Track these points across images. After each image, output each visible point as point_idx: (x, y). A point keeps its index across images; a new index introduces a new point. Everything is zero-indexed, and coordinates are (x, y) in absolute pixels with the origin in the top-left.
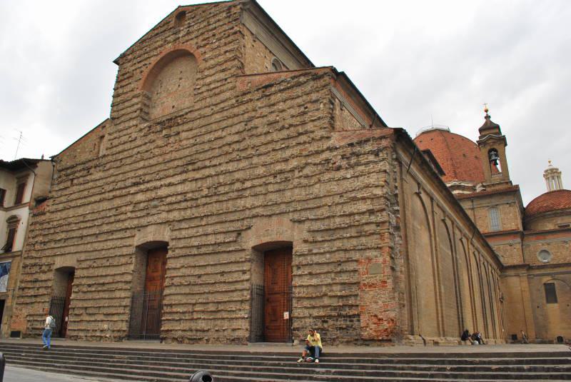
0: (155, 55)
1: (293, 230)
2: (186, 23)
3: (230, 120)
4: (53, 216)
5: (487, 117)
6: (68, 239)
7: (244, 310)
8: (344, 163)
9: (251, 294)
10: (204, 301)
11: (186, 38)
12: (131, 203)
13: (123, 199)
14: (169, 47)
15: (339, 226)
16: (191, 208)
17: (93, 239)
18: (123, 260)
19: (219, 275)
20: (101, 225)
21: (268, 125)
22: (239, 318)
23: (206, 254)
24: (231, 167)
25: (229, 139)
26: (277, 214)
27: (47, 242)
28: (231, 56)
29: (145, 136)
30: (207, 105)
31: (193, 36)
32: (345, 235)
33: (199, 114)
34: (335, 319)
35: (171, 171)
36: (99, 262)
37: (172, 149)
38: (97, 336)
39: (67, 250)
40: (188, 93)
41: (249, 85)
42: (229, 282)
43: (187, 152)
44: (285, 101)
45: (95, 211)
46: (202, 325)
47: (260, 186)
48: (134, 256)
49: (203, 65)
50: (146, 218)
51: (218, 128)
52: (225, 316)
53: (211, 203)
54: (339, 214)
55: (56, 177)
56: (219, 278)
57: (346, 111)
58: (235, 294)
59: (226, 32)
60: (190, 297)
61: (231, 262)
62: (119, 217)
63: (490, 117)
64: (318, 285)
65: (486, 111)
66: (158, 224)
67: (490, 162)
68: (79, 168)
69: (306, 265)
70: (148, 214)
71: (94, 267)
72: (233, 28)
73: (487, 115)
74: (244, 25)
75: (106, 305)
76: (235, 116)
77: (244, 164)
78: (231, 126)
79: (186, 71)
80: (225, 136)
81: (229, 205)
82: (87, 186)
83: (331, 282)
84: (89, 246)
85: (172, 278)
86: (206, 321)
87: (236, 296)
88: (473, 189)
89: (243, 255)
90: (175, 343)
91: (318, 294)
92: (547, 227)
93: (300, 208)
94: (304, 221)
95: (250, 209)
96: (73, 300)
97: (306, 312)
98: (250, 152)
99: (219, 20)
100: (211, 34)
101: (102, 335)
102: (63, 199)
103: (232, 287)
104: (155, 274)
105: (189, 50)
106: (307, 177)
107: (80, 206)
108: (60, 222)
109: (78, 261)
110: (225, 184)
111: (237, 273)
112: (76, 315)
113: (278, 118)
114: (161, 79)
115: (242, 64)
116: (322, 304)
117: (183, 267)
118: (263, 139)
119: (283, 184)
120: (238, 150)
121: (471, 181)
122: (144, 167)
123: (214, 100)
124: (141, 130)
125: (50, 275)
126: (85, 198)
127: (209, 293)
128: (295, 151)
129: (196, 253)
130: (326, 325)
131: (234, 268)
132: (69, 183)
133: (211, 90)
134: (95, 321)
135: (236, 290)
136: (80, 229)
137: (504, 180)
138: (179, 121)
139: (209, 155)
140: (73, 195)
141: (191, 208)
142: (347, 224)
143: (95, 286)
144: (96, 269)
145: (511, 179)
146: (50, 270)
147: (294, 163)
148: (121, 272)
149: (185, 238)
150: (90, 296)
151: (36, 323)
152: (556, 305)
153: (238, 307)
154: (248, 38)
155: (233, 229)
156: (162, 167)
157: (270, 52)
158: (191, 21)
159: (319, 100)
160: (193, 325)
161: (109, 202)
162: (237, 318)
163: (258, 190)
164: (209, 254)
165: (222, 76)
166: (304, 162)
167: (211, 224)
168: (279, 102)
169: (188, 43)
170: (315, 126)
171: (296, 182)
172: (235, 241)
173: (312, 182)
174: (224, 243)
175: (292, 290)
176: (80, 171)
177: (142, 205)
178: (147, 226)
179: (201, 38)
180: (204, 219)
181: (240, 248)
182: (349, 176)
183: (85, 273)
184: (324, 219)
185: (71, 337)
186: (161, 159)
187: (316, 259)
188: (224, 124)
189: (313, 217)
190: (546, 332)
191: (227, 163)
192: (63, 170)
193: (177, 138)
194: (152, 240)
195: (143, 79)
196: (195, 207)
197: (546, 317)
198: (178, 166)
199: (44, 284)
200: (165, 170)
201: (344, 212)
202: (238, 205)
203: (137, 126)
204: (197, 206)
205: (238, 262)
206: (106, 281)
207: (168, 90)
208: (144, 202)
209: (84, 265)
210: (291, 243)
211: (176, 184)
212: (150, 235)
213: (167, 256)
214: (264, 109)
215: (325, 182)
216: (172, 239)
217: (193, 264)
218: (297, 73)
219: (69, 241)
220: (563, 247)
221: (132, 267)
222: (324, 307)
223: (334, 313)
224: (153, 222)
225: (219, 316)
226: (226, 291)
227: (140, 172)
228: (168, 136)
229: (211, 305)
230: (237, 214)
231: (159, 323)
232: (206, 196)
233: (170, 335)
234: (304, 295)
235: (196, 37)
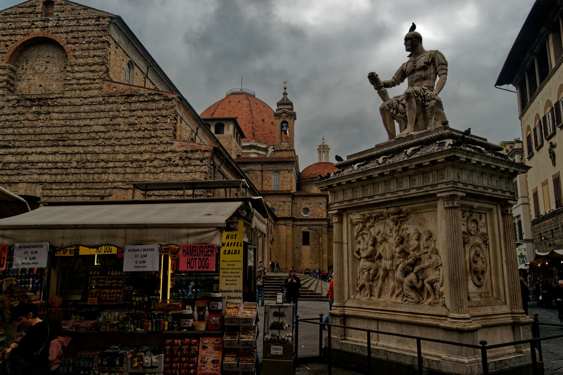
0: (21, 35)
2: (55, 14)
3: (98, 113)
5: (285, 94)
8: (181, 163)
11: (55, 30)
14: (37, 32)
16: (61, 174)
21: (129, 125)
24: (97, 149)
25: (96, 128)
28: (99, 61)
29: (14, 107)
30: (77, 96)
31: (63, 30)
33: (69, 102)
35: (42, 142)
37: (42, 124)
40: (56, 78)
41: (114, 89)
43: (57, 130)
44: (142, 110)
49: (73, 61)
50: (17, 177)
51: (87, 117)
53: (80, 173)
54: (174, 194)
57: (184, 122)
59: (95, 38)
63: (287, 94)
65: (285, 89)
66: (29, 182)
67: (282, 131)
70: (20, 174)
72: (101, 37)
73: (285, 92)
74: (110, 36)
76: (102, 111)
77: (107, 149)
78: (99, 118)
79: (53, 57)
80: (92, 125)
88: (266, 150)
92: (313, 189)
95: (111, 182)
98: (113, 141)
99: (88, 25)
100: (81, 34)
105: (59, 42)
106: (155, 167)
110: (92, 162)
113: (136, 121)
114: (26, 56)
115: (108, 68)
118: (123, 134)
119: (138, 169)
120: (104, 138)
121: (266, 143)
122: (13, 134)
123: (83, 93)
124: (8, 101)
128: (148, 148)
133: (81, 84)
137: (290, 148)
138: (50, 103)
139: (78, 136)
141: (61, 174)
145: (295, 148)
147: (146, 156)
152: (308, 247)
154: (113, 45)
156: (33, 137)
157: (127, 55)
158: (60, 15)
159: (167, 116)
163: (119, 170)
165: (91, 75)
166: (153, 156)
167: (79, 189)
168: (138, 110)
169: (57, 35)
170: (163, 134)
171: (147, 169)
173: (159, 171)
177: (12, 166)
178: (17, 183)
179: (71, 35)
180: (73, 184)
182: (183, 171)
186: (31, 131)
188: (92, 115)
190: (300, 265)
191: (94, 146)
193: (48, 117)
195: (10, 54)
196: (65, 174)
197: (301, 255)
198: (49, 140)
200: (36, 140)
201: (178, 193)
203: (4, 96)
204: (69, 174)
207: (34, 69)
208: (14, 163)
214: (126, 112)
215: (167, 172)
216: (44, 196)
218: (153, 92)
220: (319, 207)
224: (24, 180)
228: (39, 113)
230: (101, 184)
232: (75, 168)
235: (66, 33)
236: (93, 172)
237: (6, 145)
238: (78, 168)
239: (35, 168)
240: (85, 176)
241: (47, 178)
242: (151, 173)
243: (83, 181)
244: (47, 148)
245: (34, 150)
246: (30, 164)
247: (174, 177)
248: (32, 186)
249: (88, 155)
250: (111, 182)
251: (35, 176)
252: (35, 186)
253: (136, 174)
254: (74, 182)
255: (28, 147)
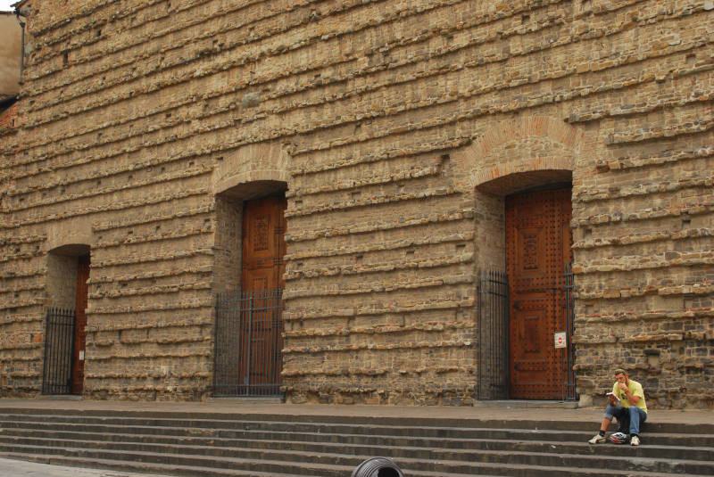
1: (570, 142)
4: (33, 136)
6: (69, 185)
7: (463, 328)
9: (478, 293)
10: (374, 310)
12: (199, 98)
13: (181, 89)
15: (684, 130)
16: (331, 102)
17: (122, 183)
18: (190, 226)
19: (403, 253)
20: (138, 150)
22: (453, 346)
23: (372, 206)
26: (532, 108)
27: (27, 194)
32: (700, 151)
34: (675, 347)
35: (282, 19)
36: (139, 233)
38: (148, 391)
39: (70, 209)
42: (426, 268)
45: (122, 121)
46: (369, 362)
47: (491, 41)
48: (213, 217)
50: (234, 131)
52: (422, 343)
53: (377, 89)
54: (684, 100)
55: (29, 49)
56: (404, 259)
58: (441, 294)
60: (339, 302)
61: (430, 223)
62: (175, 131)
64: (633, 270)
66: (260, 142)
68: (79, 25)
69: (607, 224)
70: (240, 120)
71: (129, 244)
75: (162, 324)
81: (420, 92)
82: (99, 65)
83: (667, 263)
84: (115, 197)
85: (299, 261)
86: (379, 354)
87: (443, 299)
89: (455, 205)
90: (313, 403)
91: (635, 291)
93: (587, 91)
94: (598, 121)
95: (467, 99)
96: (91, 314)
97: (608, 333)
101: (159, 387)
102: (51, 97)
103: (434, 279)
104: (262, 255)
107: (87, 111)
108: (50, 149)
109: (95, 232)
110: (408, 44)
111: (443, 247)
112: (100, 346)
116: (645, 314)
117: (320, 236)
119: (545, 34)
125: (40, 265)
126: (97, 92)
127: (383, 292)
129: (349, 204)
130: (654, 362)
131: (437, 235)
132: (59, 61)
134: (141, 358)
135: (443, 285)
136: (93, 161)
140: (71, 88)
141: (331, 102)
142: (705, 123)
143: (136, 284)
144: (134, 248)
146: (38, 254)
148: (188, 253)
149: (322, 172)
150: (125, 305)
151: (17, 365)
153: (448, 323)
155: (429, 147)
160: (351, 363)
161: (151, 98)
162: (447, 347)
163: (485, 52)
164: (378, 205)
171: (576, 27)
172: (436, 175)
173: (617, 24)
174: (412, 179)
175: (571, 282)
176: (80, 33)
177: (223, 103)
180: (363, 126)
181: (448, 190)
183: (113, 256)
184: (646, 114)
185: (93, 393)
187: (628, 210)
189: (620, 111)
192: (43, 33)
194: (250, 180)
196: (340, 100)
199: (29, 284)
200: (269, 18)
201: (697, 95)
202: (439, 90)
204: (347, 98)
205: (446, 222)
206: (159, 274)
208: (227, 94)
209: (110, 239)
210: (571, 172)
211: (295, 50)
212: (246, 168)
213: (286, 215)
215: (647, 24)
216: (295, 176)
217: (342, 229)
219: (73, 189)
221: (211, 241)
222: (649, 320)
223: (674, 335)
225: (406, 342)
226: (421, 289)
227: (213, 27)
229: (388, 318)
230: (439, 111)
231: (277, 359)
232: (365, 74)
233: (301, 385)
234: (601, 294)
236: (411, 77)
237: (207, 50)
238: (373, 74)
239: (270, 99)
240: (393, 92)
241: (298, 121)
242: (592, 39)
243: (387, 111)
244: (294, 32)
245: (265, 47)
246: (261, 88)
247: (677, 35)
248: (267, 152)
249: (396, 25)
250: (467, 99)
251: (273, 122)
252: (274, 151)
253: (542, 55)
254: (365, 119)
255: (253, 42)
